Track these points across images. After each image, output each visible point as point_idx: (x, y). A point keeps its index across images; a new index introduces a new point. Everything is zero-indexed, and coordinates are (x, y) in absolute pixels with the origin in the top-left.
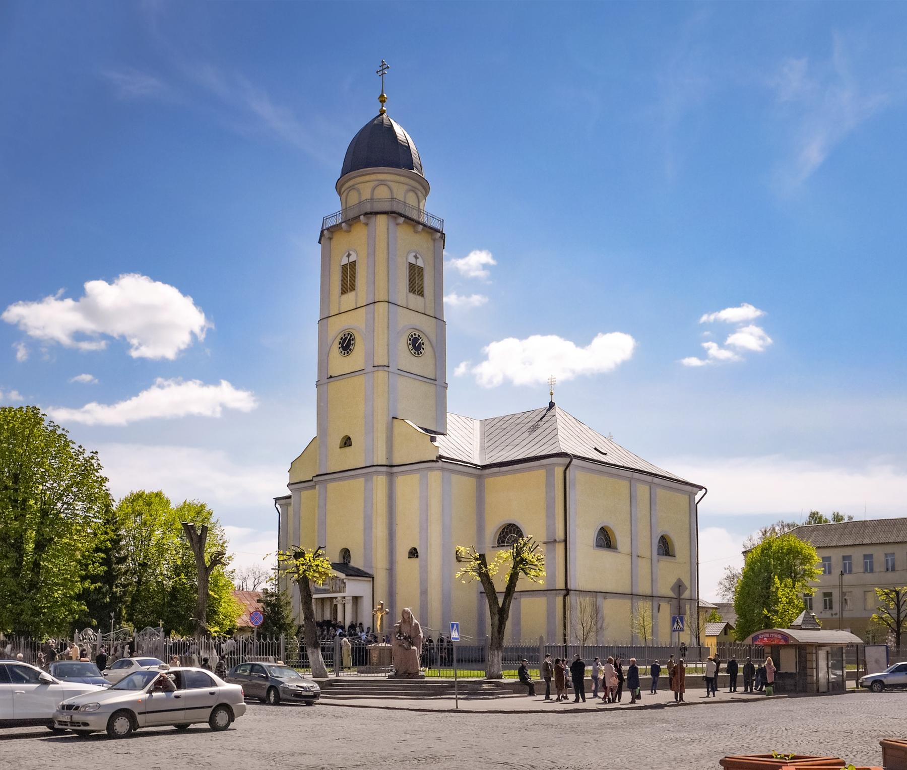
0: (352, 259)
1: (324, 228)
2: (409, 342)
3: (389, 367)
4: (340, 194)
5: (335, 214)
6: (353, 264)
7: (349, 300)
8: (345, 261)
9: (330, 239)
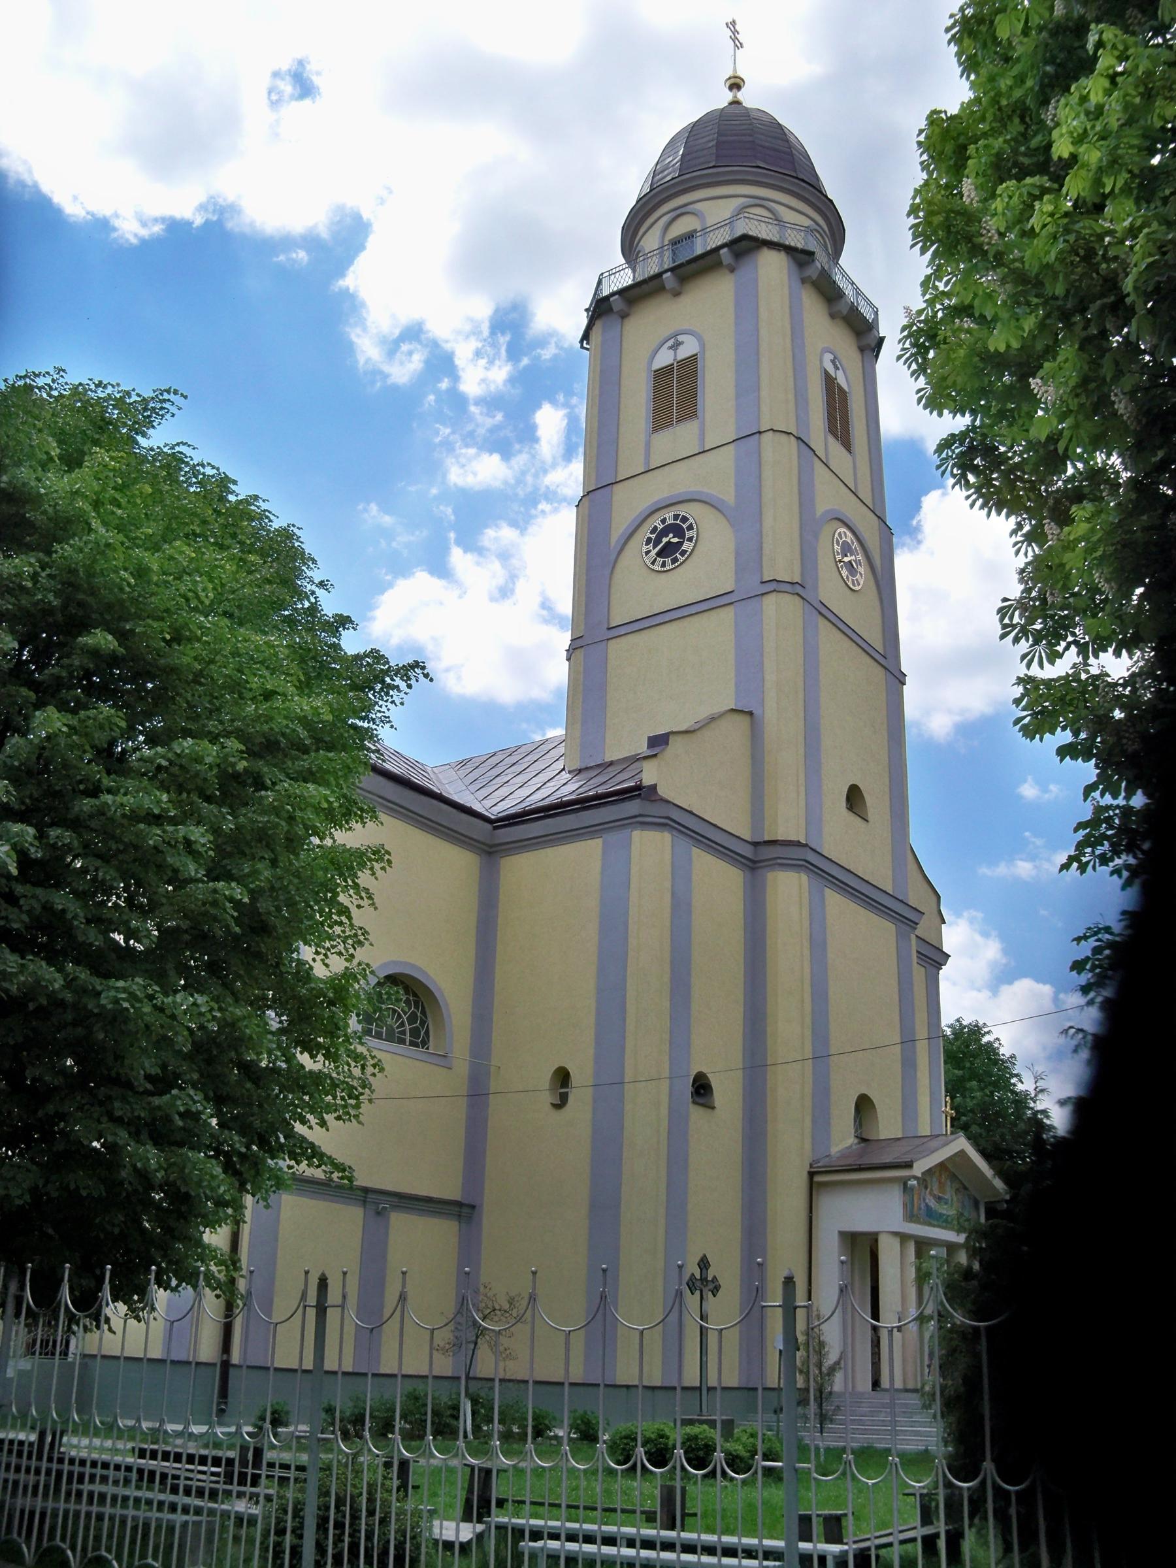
0: (683, 353)
1: (605, 293)
7: (682, 437)
8: (665, 358)
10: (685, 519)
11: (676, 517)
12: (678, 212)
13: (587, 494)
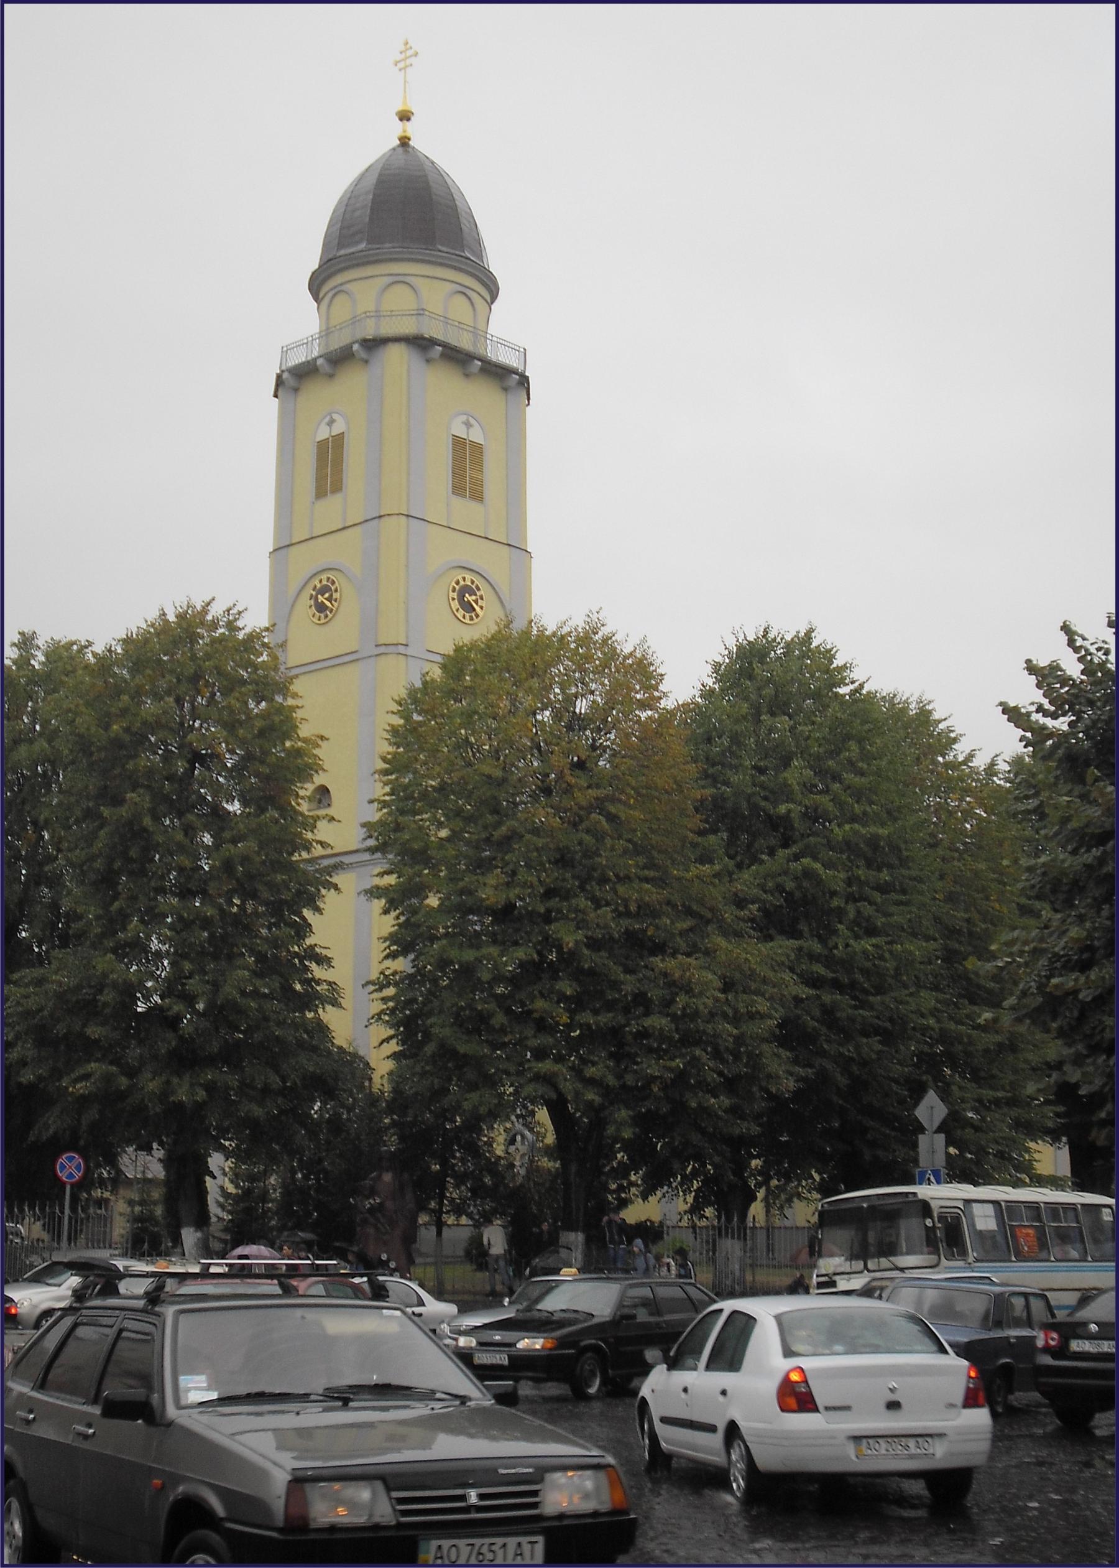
1: (284, 368)
2: (451, 594)
3: (407, 645)
4: (316, 298)
5: (305, 341)
6: (338, 441)
7: (331, 511)
8: (323, 433)
9: (296, 390)
10: (333, 583)
11: (328, 579)
12: (336, 290)
13: (275, 550)
